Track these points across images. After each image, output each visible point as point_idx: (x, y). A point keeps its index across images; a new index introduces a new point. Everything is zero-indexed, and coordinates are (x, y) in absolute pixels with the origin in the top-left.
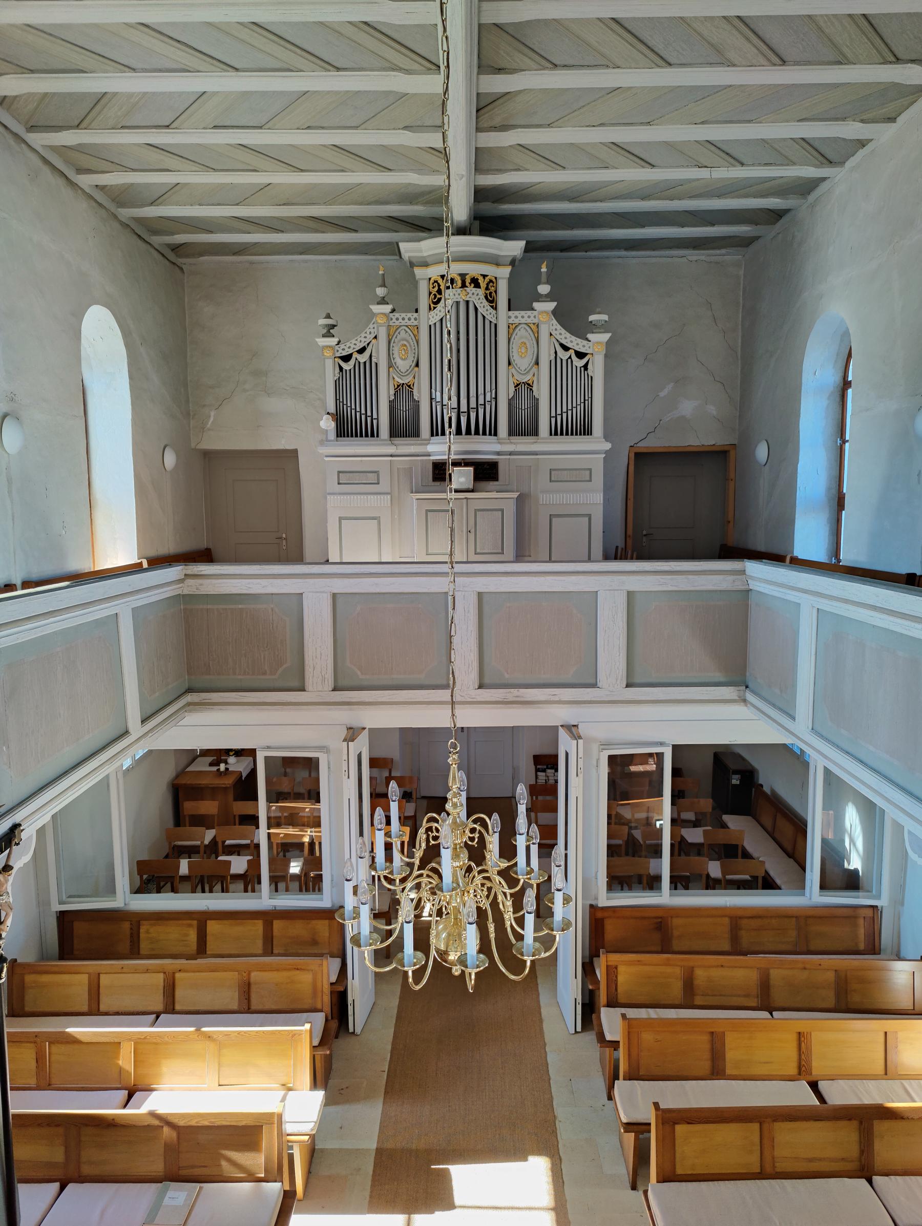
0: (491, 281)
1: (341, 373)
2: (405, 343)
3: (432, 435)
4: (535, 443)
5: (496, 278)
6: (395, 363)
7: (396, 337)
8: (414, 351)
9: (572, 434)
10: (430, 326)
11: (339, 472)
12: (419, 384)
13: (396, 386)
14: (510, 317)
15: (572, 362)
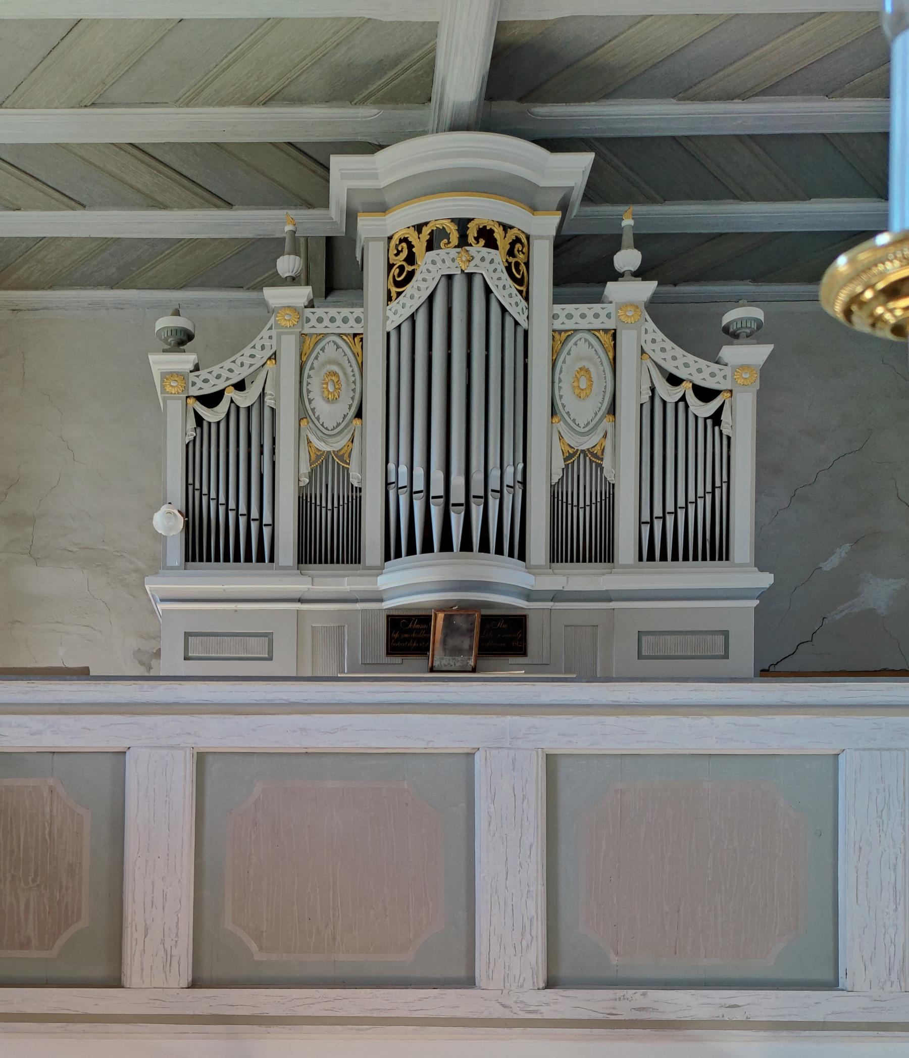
0: (517, 240)
1: (198, 430)
2: (335, 368)
3: (387, 558)
6: (313, 410)
7: (316, 358)
8: (353, 387)
10: (388, 334)
11: (187, 635)
12: (362, 453)
13: (313, 457)
14: (555, 317)
15: (687, 407)
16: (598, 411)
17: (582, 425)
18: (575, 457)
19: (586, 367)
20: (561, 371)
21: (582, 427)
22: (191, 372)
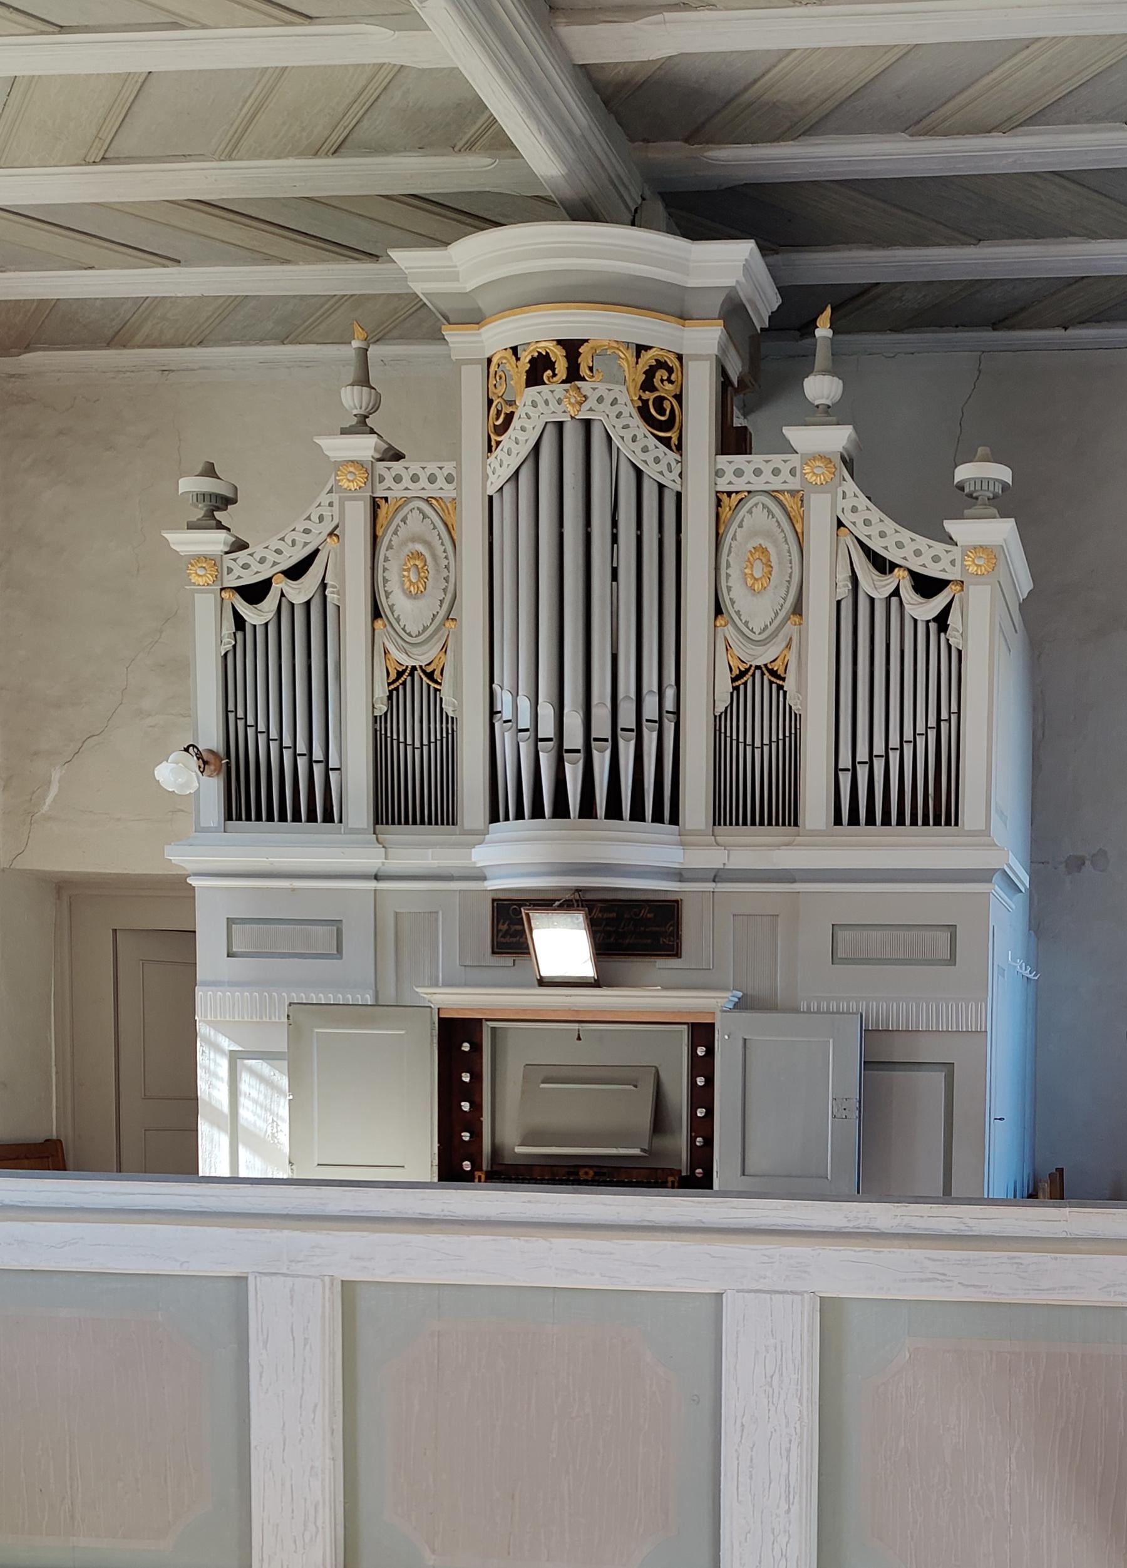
2: (420, 548)
3: (494, 818)
5: (680, 358)
6: (391, 607)
8: (445, 573)
12: (458, 667)
17: (757, 631)
18: (747, 676)
21: (757, 633)
22: (227, 553)
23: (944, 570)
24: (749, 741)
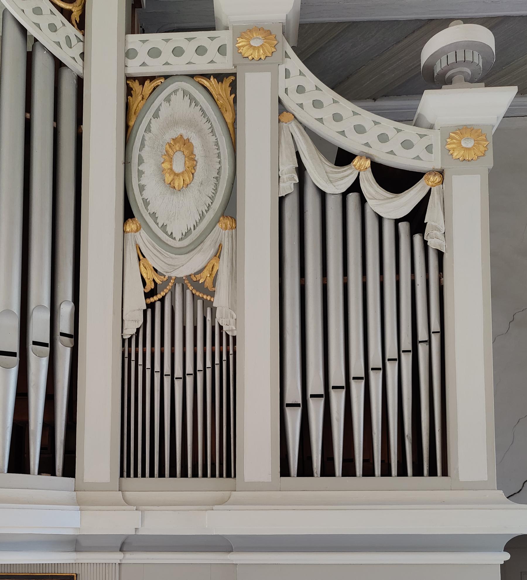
4: (222, 502)
9: (368, 472)
14: (130, 54)
15: (363, 201)
16: (207, 211)
17: (178, 236)
18: (166, 291)
19: (185, 138)
20: (143, 145)
21: (177, 239)
23: (418, 158)
24: (167, 370)
